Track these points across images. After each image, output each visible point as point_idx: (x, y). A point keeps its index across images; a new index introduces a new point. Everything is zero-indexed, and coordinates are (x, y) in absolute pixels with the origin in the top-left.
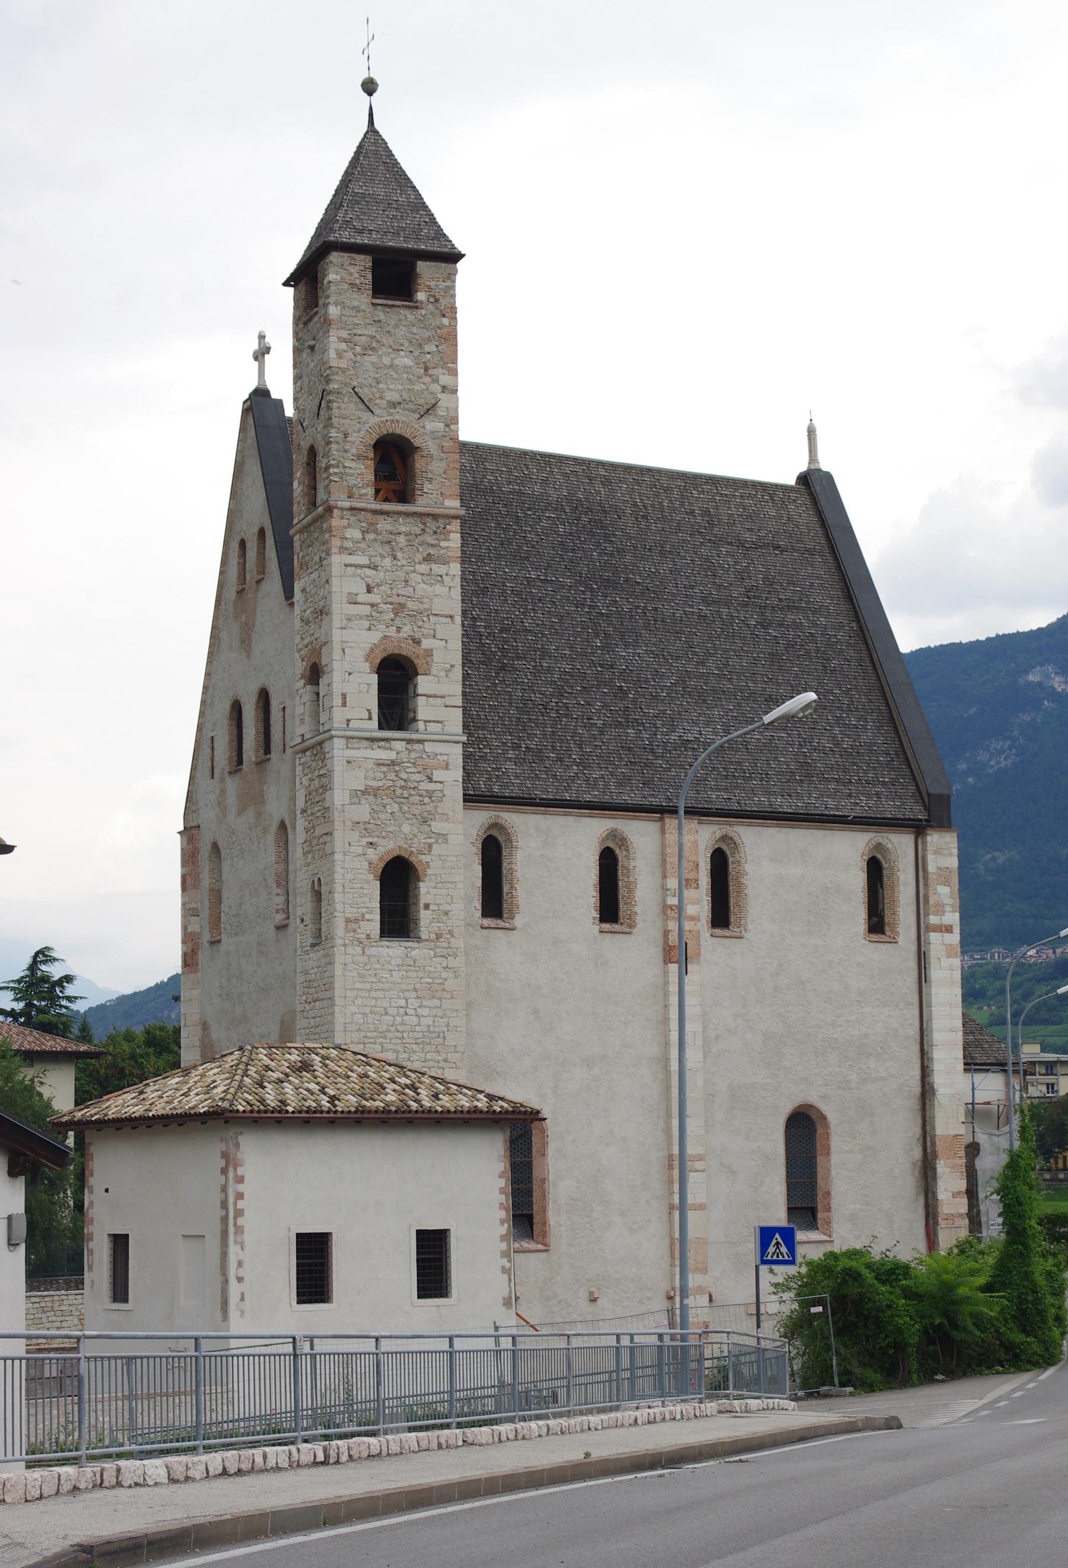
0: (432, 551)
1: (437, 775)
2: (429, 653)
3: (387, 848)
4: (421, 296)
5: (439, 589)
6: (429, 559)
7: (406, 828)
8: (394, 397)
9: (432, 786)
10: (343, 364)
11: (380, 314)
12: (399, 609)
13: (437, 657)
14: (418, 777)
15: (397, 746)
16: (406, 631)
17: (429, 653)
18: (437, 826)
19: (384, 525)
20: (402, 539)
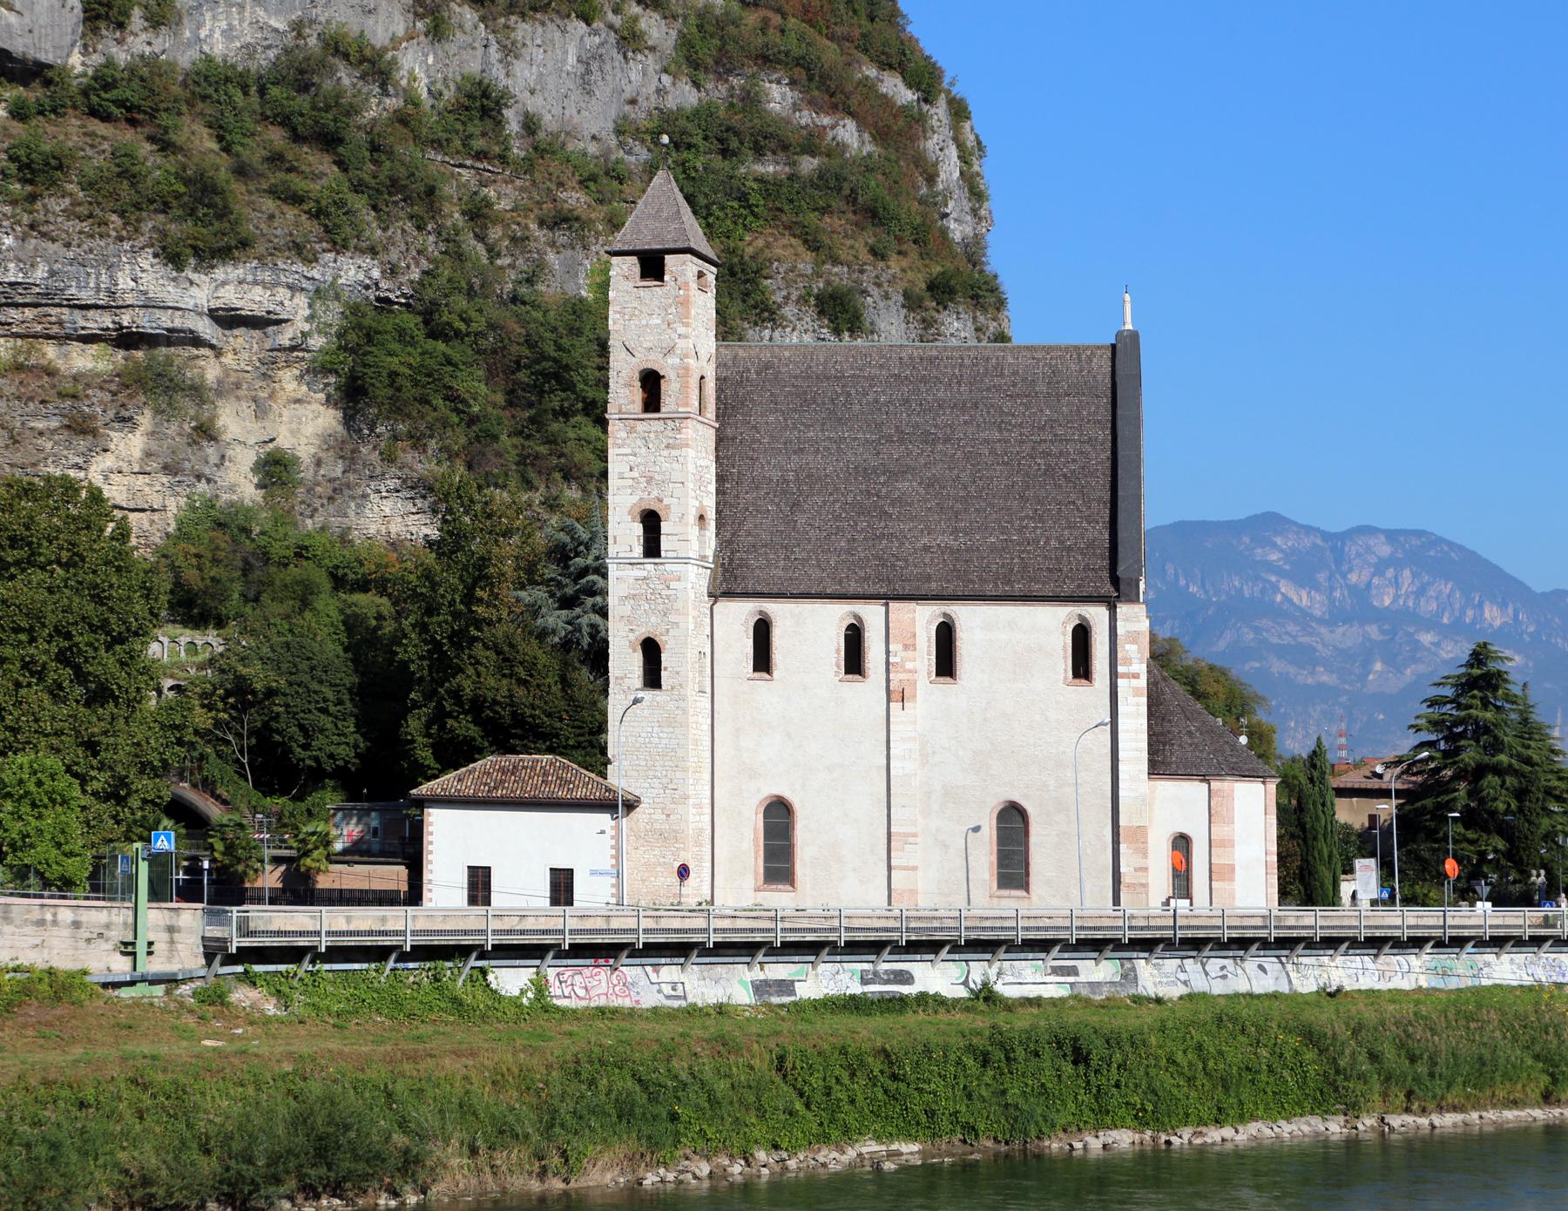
0: (671, 441)
1: (673, 585)
2: (668, 507)
3: (642, 632)
4: (666, 278)
5: (675, 465)
6: (668, 446)
7: (653, 619)
9: (670, 592)
10: (616, 327)
11: (642, 292)
12: (650, 480)
13: (673, 509)
14: (661, 587)
15: (650, 566)
16: (655, 493)
17: (668, 507)
18: (672, 618)
19: (641, 426)
20: (652, 435)
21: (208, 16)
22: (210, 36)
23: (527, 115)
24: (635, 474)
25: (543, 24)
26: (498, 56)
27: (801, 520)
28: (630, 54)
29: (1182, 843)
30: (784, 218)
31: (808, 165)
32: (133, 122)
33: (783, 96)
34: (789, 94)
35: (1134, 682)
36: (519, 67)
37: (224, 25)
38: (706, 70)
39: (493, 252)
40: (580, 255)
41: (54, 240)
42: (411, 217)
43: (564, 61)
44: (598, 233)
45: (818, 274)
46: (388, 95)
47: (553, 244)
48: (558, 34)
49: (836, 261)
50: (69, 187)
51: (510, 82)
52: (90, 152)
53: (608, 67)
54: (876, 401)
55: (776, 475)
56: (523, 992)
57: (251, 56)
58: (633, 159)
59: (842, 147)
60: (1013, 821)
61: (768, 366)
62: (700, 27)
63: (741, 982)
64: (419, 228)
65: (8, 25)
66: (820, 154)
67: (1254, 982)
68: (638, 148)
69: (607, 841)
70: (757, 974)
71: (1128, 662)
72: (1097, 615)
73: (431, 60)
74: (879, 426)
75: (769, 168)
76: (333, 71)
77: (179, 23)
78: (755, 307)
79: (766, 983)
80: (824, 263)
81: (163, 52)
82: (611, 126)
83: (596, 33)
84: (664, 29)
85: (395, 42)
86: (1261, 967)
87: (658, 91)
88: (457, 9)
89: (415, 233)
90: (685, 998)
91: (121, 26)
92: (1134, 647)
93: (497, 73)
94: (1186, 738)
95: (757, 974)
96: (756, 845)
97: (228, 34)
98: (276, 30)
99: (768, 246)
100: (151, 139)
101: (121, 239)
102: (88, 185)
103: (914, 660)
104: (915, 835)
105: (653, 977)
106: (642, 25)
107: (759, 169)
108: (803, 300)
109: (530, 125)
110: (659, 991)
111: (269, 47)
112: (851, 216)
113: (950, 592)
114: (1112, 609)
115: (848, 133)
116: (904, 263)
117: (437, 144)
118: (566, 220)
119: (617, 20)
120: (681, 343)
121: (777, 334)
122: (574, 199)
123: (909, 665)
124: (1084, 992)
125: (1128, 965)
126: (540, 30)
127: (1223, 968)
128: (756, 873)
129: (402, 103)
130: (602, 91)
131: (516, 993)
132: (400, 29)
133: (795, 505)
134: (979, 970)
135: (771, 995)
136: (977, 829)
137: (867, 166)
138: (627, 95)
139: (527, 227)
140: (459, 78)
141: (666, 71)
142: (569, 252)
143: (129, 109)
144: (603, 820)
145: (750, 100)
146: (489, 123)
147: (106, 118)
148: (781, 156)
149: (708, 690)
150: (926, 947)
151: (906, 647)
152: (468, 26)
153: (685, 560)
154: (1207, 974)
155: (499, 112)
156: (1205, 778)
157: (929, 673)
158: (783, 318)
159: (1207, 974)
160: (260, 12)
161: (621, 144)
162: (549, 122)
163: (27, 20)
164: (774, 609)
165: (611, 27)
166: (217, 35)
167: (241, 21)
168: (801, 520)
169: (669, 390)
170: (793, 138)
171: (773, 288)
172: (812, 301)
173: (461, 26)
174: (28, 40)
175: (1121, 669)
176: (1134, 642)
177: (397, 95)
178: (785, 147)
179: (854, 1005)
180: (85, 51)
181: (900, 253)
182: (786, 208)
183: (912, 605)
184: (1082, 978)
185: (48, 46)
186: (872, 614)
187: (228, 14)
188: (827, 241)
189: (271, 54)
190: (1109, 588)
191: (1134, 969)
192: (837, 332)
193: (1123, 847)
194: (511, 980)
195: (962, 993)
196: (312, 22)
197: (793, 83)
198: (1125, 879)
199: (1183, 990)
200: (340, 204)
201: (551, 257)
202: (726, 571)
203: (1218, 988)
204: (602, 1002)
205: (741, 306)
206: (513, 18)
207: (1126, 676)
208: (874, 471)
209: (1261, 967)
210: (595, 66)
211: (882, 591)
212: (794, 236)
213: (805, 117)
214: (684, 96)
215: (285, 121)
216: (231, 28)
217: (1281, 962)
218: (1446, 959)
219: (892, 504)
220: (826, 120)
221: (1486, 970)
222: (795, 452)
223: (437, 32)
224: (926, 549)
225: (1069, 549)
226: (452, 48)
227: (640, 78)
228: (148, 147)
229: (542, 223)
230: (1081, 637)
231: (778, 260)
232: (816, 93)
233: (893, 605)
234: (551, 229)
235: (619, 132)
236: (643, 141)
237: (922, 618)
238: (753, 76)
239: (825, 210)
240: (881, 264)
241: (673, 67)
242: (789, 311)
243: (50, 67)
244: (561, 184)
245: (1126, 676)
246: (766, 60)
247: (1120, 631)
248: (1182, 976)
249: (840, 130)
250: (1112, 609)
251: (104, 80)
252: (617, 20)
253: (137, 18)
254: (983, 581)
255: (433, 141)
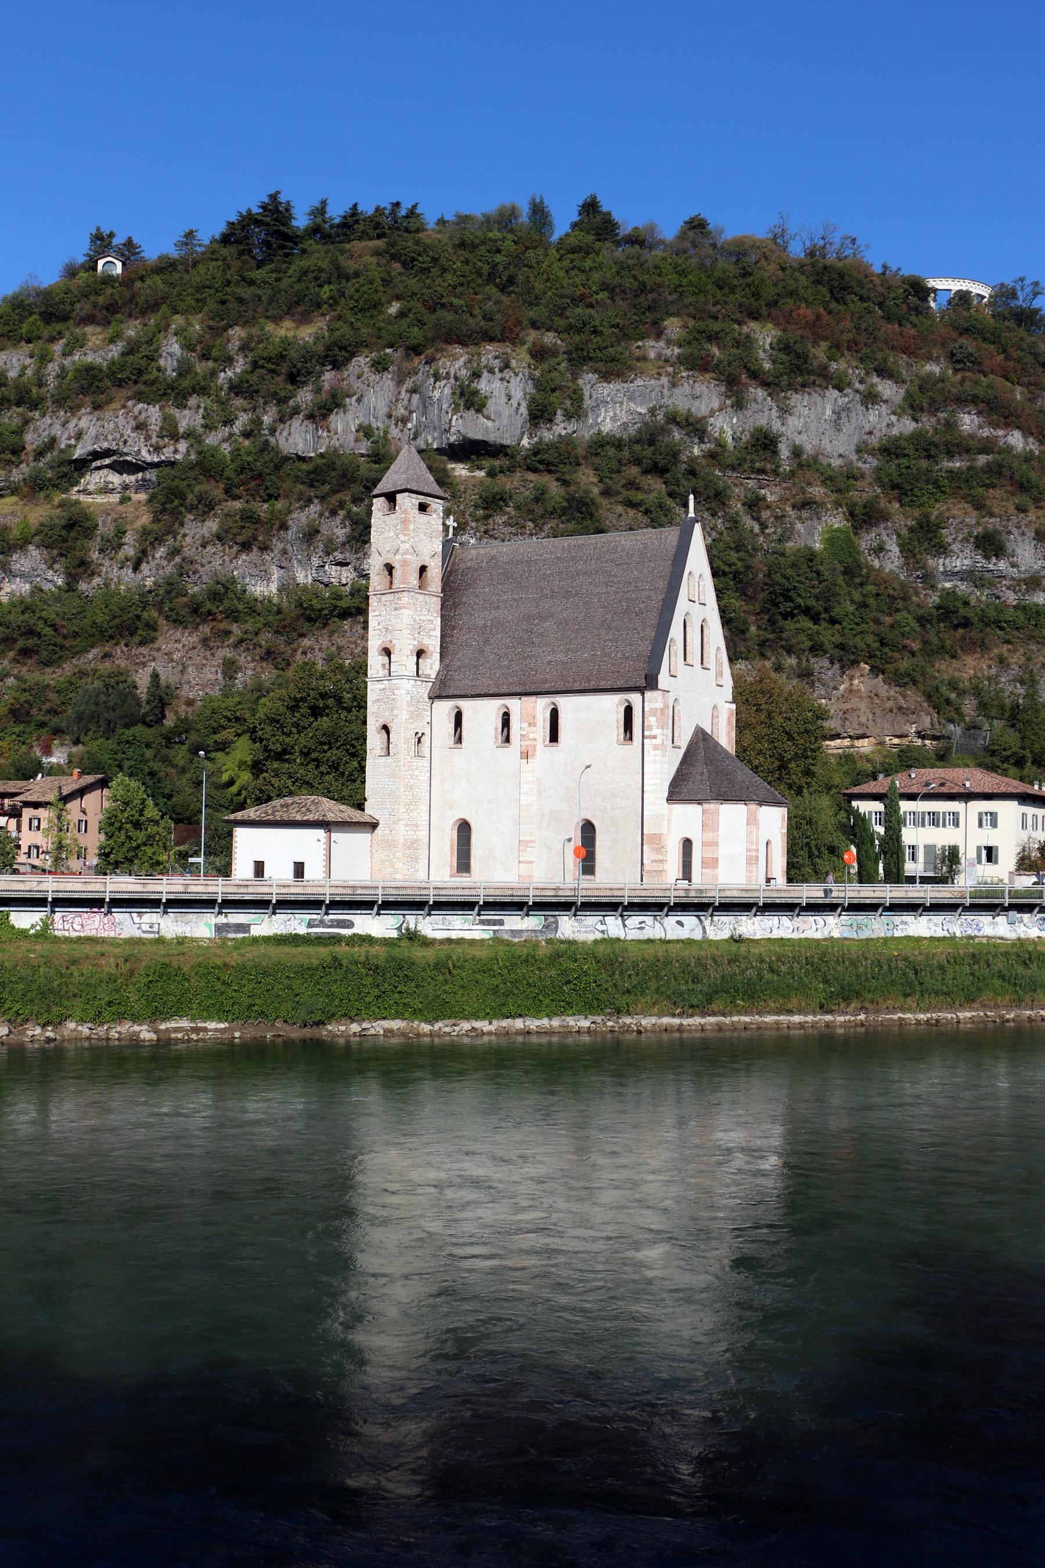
1: (396, 692)
3: (381, 722)
5: (398, 620)
8: (387, 549)
16: (389, 637)
18: (395, 712)
21: (603, 410)
22: (603, 421)
23: (795, 446)
24: (380, 627)
25: (809, 394)
26: (777, 414)
27: (487, 649)
28: (870, 406)
29: (687, 844)
30: (961, 492)
31: (982, 460)
32: (550, 472)
33: (972, 421)
34: (976, 419)
35: (654, 741)
36: (792, 421)
37: (611, 414)
38: (922, 410)
39: (764, 526)
40: (815, 523)
41: (496, 539)
42: (708, 510)
43: (824, 413)
44: (828, 510)
45: (978, 524)
46: (704, 443)
47: (800, 518)
48: (819, 399)
49: (992, 515)
50: (508, 509)
51: (784, 429)
52: (522, 489)
53: (853, 415)
54: (544, 574)
55: (481, 623)
56: (33, 926)
57: (625, 430)
58: (867, 466)
59: (1009, 449)
60: (588, 829)
61: (493, 558)
62: (921, 387)
63: (207, 924)
64: (713, 515)
65: (487, 427)
66: (993, 453)
67: (669, 932)
68: (870, 459)
69: (322, 846)
70: (222, 920)
71: (650, 728)
72: (635, 698)
73: (735, 421)
74: (542, 589)
75: (957, 464)
76: (670, 432)
77: (586, 416)
78: (935, 546)
79: (227, 925)
80: (984, 517)
81: (574, 432)
82: (853, 448)
83: (846, 396)
84: (895, 389)
85: (712, 413)
86: (680, 923)
87: (888, 425)
88: (753, 390)
89: (710, 518)
90: (158, 933)
91: (551, 421)
92: (654, 719)
93: (776, 426)
94: (699, 778)
95: (222, 920)
96: (452, 849)
97: (614, 419)
98: (640, 414)
99: (948, 509)
100: (558, 480)
101: (531, 535)
102: (518, 508)
103: (534, 732)
104: (531, 842)
105: (137, 919)
106: (880, 388)
107: (950, 464)
108: (966, 540)
109: (797, 452)
110: (139, 928)
111: (636, 423)
112: (1009, 488)
113: (555, 689)
114: (643, 694)
115: (1016, 440)
116: (1040, 513)
117: (734, 468)
118: (808, 504)
119: (861, 387)
120: (403, 546)
121: (947, 561)
122: (817, 491)
123: (531, 736)
124: (506, 937)
125: (552, 919)
126: (807, 397)
127: (641, 923)
128: (451, 866)
129: (713, 446)
130: (848, 428)
131: (28, 927)
132: (716, 405)
133: (486, 641)
134: (415, 921)
135: (228, 932)
136: (570, 840)
137: (1028, 457)
138: (867, 429)
139: (784, 510)
140: (752, 429)
141: (894, 413)
142: (809, 522)
143: (547, 465)
144: (320, 833)
145: (950, 425)
146: (768, 454)
147: (535, 470)
148: (965, 456)
149: (428, 756)
150: (364, 905)
151: (530, 725)
152: (760, 399)
153: (401, 677)
154: (625, 926)
155: (776, 446)
156: (699, 802)
157: (544, 741)
158: (951, 551)
159: (625, 926)
160: (632, 405)
161: (860, 458)
162: (809, 448)
163: (497, 424)
164: (465, 705)
165: (857, 391)
166: (608, 420)
167: (621, 411)
168: (487, 649)
169: (397, 573)
170: (972, 443)
171: (947, 534)
172: (972, 540)
173: (755, 400)
174: (497, 434)
175: (646, 733)
176: (654, 715)
177: (709, 442)
178: (968, 451)
179: (294, 940)
180: (530, 437)
181: (1037, 507)
182: (963, 486)
183: (533, 698)
184: (506, 927)
185: (508, 436)
186: (514, 705)
187: (614, 408)
188: (988, 503)
189: (636, 426)
190: (642, 682)
191: (556, 922)
192: (987, 557)
193: (645, 847)
194: (24, 920)
195: (394, 934)
196: (661, 407)
197: (979, 413)
198: (646, 868)
199: (599, 936)
200: (661, 506)
201: (799, 526)
202: (442, 682)
203: (633, 935)
204: (93, 933)
205: (926, 544)
206: (790, 393)
207: (650, 737)
208: (534, 615)
209: (680, 923)
210: (843, 415)
211: (519, 690)
212: (967, 502)
213: (986, 432)
214: (907, 426)
215: (638, 461)
216: (615, 415)
217: (700, 920)
218: (861, 918)
219: (537, 637)
220: (1001, 433)
221: (900, 927)
222: (495, 609)
223: (739, 405)
224: (550, 662)
225: (628, 658)
226: (748, 413)
227: (876, 419)
228: (555, 483)
229: (794, 507)
230: (629, 711)
231: (953, 517)
232: (995, 417)
233: (524, 698)
234: (799, 510)
235: (858, 451)
236: (874, 455)
237: (541, 706)
238: (953, 411)
239: (993, 486)
240: (1022, 515)
241: (899, 411)
242: (955, 547)
243: (508, 447)
244: (809, 484)
245: (650, 737)
246: (963, 401)
247: (646, 709)
248: (603, 927)
249: (1009, 438)
250: (643, 694)
251: (536, 451)
252: (861, 387)
253: (559, 416)
254: (575, 681)
255: (729, 466)
